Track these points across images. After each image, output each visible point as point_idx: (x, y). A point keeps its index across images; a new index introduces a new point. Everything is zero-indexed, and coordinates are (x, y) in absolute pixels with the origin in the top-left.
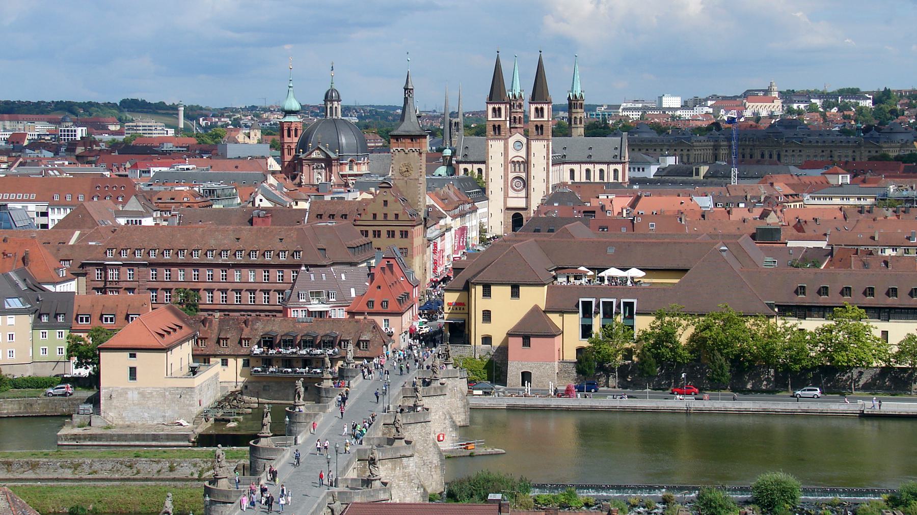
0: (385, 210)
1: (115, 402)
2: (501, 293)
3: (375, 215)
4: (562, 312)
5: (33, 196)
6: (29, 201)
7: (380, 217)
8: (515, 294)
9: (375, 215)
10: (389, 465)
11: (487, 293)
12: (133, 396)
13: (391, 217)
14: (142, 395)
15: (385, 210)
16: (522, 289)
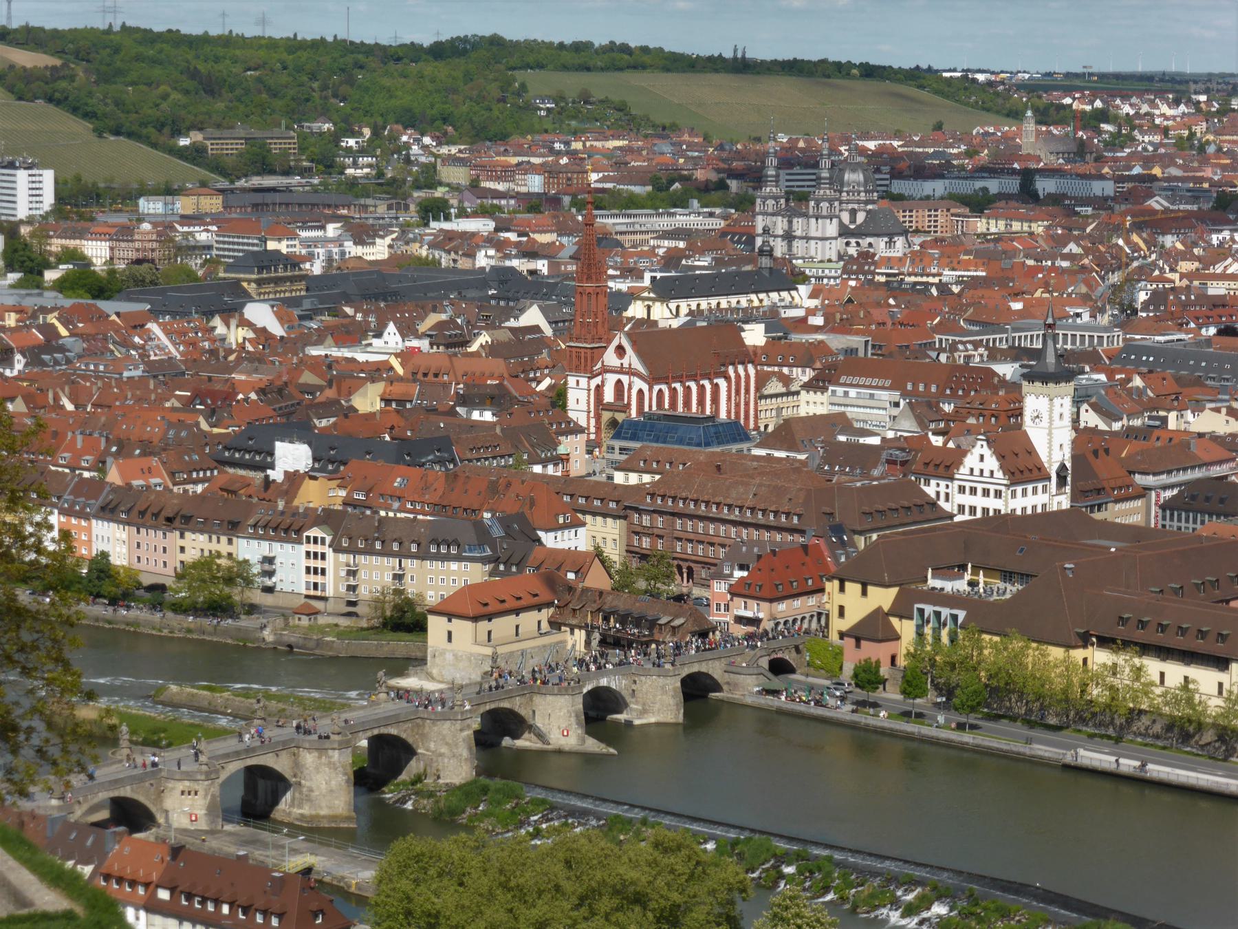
0: (982, 465)
1: (437, 660)
2: (853, 588)
3: (972, 470)
4: (901, 617)
5: (888, 383)
6: (883, 388)
7: (977, 472)
8: (864, 593)
9: (972, 470)
10: (316, 754)
11: (842, 589)
12: (449, 657)
13: (986, 473)
14: (455, 656)
15: (982, 465)
16: (870, 589)
